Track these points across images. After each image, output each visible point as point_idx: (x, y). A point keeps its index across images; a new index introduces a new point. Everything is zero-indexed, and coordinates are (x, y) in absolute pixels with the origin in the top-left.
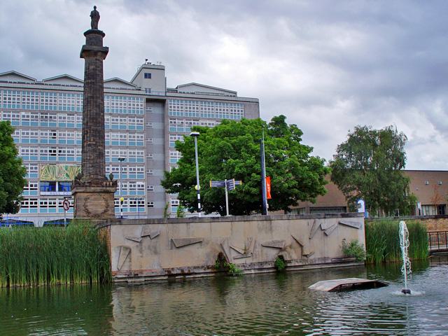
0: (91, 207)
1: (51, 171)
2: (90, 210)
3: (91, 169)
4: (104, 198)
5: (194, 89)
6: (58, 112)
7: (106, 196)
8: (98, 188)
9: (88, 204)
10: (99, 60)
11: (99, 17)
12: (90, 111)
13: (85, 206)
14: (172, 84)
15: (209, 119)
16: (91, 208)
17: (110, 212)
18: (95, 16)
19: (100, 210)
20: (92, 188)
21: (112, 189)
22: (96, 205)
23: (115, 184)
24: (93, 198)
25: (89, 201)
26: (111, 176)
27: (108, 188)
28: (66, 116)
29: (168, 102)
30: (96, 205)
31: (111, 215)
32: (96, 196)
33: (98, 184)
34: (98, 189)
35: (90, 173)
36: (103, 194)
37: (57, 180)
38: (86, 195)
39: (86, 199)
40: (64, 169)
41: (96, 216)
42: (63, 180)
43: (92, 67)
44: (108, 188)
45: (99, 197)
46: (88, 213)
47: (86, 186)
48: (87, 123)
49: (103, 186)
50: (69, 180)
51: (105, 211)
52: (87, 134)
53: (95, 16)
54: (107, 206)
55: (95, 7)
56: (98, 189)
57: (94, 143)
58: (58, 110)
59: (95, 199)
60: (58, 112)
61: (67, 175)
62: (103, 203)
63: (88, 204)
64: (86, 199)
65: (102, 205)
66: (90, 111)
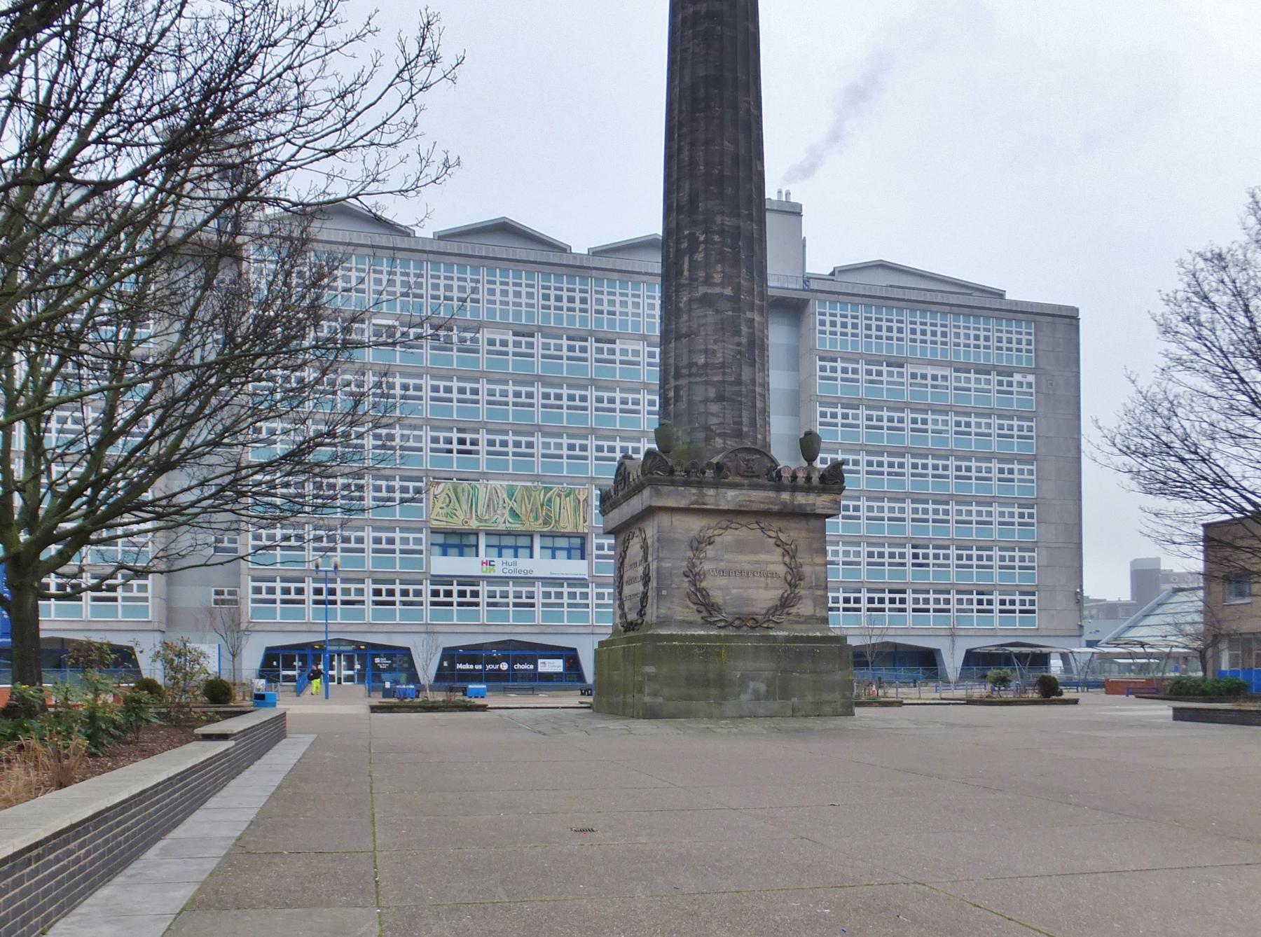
0: (723, 581)
1: (464, 499)
2: (717, 597)
3: (714, 408)
5: (881, 280)
7: (795, 533)
9: (707, 566)
12: (707, 143)
13: (693, 575)
14: (819, 263)
15: (932, 363)
16: (719, 588)
17: (805, 608)
19: (763, 596)
20: (731, 494)
21: (820, 502)
22: (740, 573)
23: (833, 479)
24: (728, 537)
25: (710, 551)
26: (809, 445)
27: (801, 499)
28: (511, 338)
29: (815, 307)
30: (740, 573)
31: (809, 620)
32: (746, 532)
34: (759, 498)
35: (707, 428)
36: (776, 524)
37: (483, 526)
38: (694, 525)
39: (699, 544)
40: (503, 495)
41: (747, 621)
42: (502, 527)
44: (801, 499)
46: (707, 606)
47: (700, 484)
48: (693, 199)
49: (779, 488)
50: (518, 527)
51: (785, 604)
52: (692, 250)
54: (795, 578)
56: (759, 498)
58: (483, 316)
59: (740, 547)
61: (514, 514)
62: (774, 561)
64: (699, 544)
65: (773, 575)
66: (707, 143)
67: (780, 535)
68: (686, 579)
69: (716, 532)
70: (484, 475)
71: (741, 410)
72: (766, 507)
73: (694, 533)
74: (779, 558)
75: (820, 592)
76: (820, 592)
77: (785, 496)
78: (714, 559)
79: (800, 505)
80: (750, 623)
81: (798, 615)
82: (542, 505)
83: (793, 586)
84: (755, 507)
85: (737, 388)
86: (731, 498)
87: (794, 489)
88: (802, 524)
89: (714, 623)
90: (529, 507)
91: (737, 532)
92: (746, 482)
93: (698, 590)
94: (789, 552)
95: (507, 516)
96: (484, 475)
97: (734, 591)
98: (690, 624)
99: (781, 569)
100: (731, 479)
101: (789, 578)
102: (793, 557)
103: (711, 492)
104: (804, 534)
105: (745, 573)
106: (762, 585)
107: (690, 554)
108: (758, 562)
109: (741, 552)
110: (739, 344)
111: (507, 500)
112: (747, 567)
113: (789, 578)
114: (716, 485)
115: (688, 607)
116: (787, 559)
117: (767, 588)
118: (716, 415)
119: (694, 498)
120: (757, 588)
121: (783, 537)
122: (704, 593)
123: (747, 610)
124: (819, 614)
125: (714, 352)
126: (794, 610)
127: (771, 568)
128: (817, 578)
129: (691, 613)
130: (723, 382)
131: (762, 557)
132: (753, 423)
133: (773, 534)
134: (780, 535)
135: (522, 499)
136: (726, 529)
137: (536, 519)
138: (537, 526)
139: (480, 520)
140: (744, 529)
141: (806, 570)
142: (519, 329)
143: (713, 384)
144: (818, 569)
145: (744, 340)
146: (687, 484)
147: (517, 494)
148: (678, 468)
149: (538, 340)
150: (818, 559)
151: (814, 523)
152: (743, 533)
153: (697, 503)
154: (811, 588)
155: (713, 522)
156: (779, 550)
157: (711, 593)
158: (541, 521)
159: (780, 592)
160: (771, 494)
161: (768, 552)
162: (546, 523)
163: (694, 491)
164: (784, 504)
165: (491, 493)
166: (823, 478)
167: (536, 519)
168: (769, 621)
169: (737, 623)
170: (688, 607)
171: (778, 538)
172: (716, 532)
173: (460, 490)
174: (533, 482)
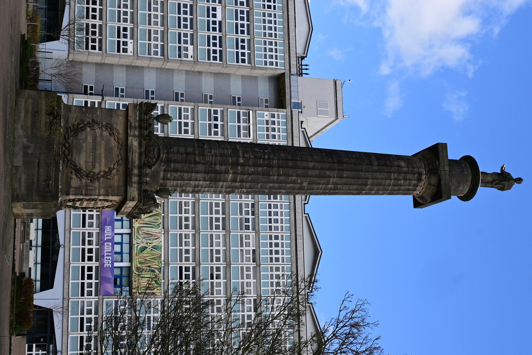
0: (90, 139)
1: (151, 219)
4: (110, 170)
6: (257, 232)
7: (116, 179)
8: (136, 157)
10: (419, 180)
11: (502, 189)
16: (87, 136)
17: (75, 182)
18: (503, 180)
19: (82, 160)
20: (136, 143)
24: (114, 143)
25: (106, 134)
27: (135, 179)
28: (251, 248)
33: (145, 152)
34: (135, 157)
36: (121, 169)
37: (135, 230)
38: (120, 127)
40: (155, 243)
42: (134, 242)
43: (403, 164)
44: (135, 179)
45: (116, 159)
46: (78, 129)
47: (140, 128)
49: (140, 168)
50: (135, 251)
51: (78, 171)
53: (503, 180)
54: (92, 177)
55: (519, 180)
56: (135, 157)
57: (241, 161)
59: (109, 150)
60: (257, 232)
61: (144, 249)
62: (101, 167)
63: (98, 131)
64: (110, 128)
65: (94, 167)
67: (115, 171)
68: (91, 121)
69: (116, 137)
70: (166, 232)
71: (182, 163)
72: (130, 161)
73: (115, 126)
74: (103, 169)
75: (84, 192)
76: (84, 192)
77: (136, 171)
78: (102, 135)
79: (131, 179)
80: (67, 152)
81: (71, 178)
82: (149, 267)
83: (87, 176)
84: (130, 155)
85: (192, 161)
86: (135, 143)
87: (140, 176)
88: (121, 184)
89: (67, 132)
90: (148, 259)
91: (116, 148)
92: (143, 150)
93: (85, 126)
94: (107, 175)
95: (142, 245)
96: (166, 232)
97: (84, 144)
98: (67, 121)
99: (97, 170)
100: (144, 143)
101: (92, 174)
102: (103, 176)
103: (137, 133)
104: (116, 184)
105: (94, 152)
106: (88, 160)
107: (104, 123)
108: (100, 159)
109: (105, 150)
110: (215, 164)
111: (152, 245)
112: (98, 153)
113: (92, 174)
114: (140, 136)
115: (76, 121)
116: (102, 173)
117: (86, 162)
118: (178, 150)
119: (133, 125)
120: (86, 157)
121: (114, 171)
122: (83, 129)
123: (74, 150)
124: (72, 190)
125: (211, 152)
126: (74, 176)
127: (97, 165)
128: (91, 190)
129: (74, 118)
130: (195, 154)
131: (103, 160)
132: (176, 170)
133: (116, 167)
134: (115, 171)
135: (153, 255)
136: (118, 142)
137: (140, 263)
138: (136, 263)
139: (139, 228)
140: (118, 152)
141: (97, 184)
142: (257, 253)
143: (194, 150)
144: (97, 191)
145: (218, 167)
146: (140, 120)
147: (156, 252)
148: (148, 117)
149: (252, 265)
150: (102, 191)
151: (123, 189)
152: (116, 151)
153: (131, 126)
154: (86, 186)
155: (122, 136)
156: (107, 170)
157: (84, 133)
158: (139, 265)
159: (84, 169)
160: (137, 163)
161: (106, 165)
162: (138, 269)
163: (137, 124)
164: (132, 170)
165: (155, 236)
166: (146, 191)
167: (140, 263)
168: (68, 161)
169: (67, 145)
170: (76, 121)
171: (114, 169)
172: (116, 137)
173: (157, 217)
174: (164, 261)
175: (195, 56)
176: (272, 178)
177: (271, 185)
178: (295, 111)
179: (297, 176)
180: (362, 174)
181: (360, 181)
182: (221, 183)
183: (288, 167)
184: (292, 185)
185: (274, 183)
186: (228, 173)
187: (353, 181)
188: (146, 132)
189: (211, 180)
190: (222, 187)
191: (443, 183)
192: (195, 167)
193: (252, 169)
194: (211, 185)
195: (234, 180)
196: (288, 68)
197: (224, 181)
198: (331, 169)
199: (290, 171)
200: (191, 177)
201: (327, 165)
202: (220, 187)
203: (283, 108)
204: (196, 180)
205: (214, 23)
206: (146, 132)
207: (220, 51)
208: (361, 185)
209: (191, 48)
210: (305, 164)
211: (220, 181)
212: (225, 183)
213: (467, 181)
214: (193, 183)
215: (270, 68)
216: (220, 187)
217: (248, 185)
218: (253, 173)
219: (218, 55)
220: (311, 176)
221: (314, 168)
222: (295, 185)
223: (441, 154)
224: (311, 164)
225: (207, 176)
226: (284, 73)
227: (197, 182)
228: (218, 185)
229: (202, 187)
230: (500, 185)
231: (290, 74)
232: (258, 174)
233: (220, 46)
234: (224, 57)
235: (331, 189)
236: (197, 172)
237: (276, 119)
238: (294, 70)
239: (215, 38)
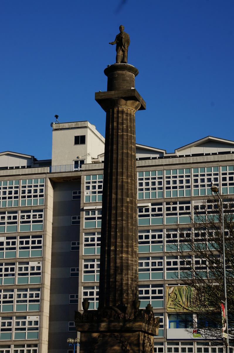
175: (38, 259)
176: (124, 225)
177: (129, 225)
178: (84, 167)
179: (122, 206)
180: (120, 157)
181: (125, 158)
182: (130, 262)
183: (116, 213)
184: (129, 210)
185: (128, 223)
186: (122, 257)
187: (125, 164)
188: (95, 318)
189: (128, 269)
190: (132, 261)
191: (124, 96)
192: (119, 282)
193: (119, 240)
194: (131, 269)
195: (127, 252)
196: (44, 176)
197: (128, 260)
198: (117, 182)
199: (119, 211)
200: (126, 284)
201: (114, 184)
202: (132, 262)
203: (81, 178)
204: (128, 280)
205: (8, 243)
206: (95, 318)
207: (33, 237)
208: (127, 157)
209: (31, 264)
210: (114, 201)
211: (128, 263)
212: (130, 259)
213: (123, 74)
214: (130, 282)
215: (45, 191)
216: (132, 262)
217: (130, 242)
218: (122, 239)
219: (36, 239)
220: (122, 195)
221: (116, 194)
222: (129, 207)
223: (103, 97)
224: (114, 196)
225: (125, 272)
226: (50, 178)
227: (130, 279)
228: (131, 263)
229: (133, 275)
230: (126, 44)
231: (50, 173)
232: (122, 235)
233: (29, 237)
234: (38, 234)
235: (132, 180)
236: (122, 279)
237: (91, 185)
238: (47, 169)
239: (22, 243)
